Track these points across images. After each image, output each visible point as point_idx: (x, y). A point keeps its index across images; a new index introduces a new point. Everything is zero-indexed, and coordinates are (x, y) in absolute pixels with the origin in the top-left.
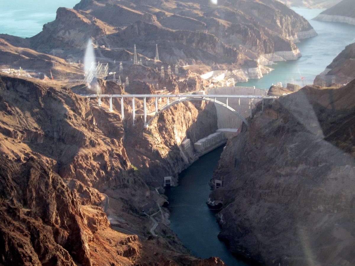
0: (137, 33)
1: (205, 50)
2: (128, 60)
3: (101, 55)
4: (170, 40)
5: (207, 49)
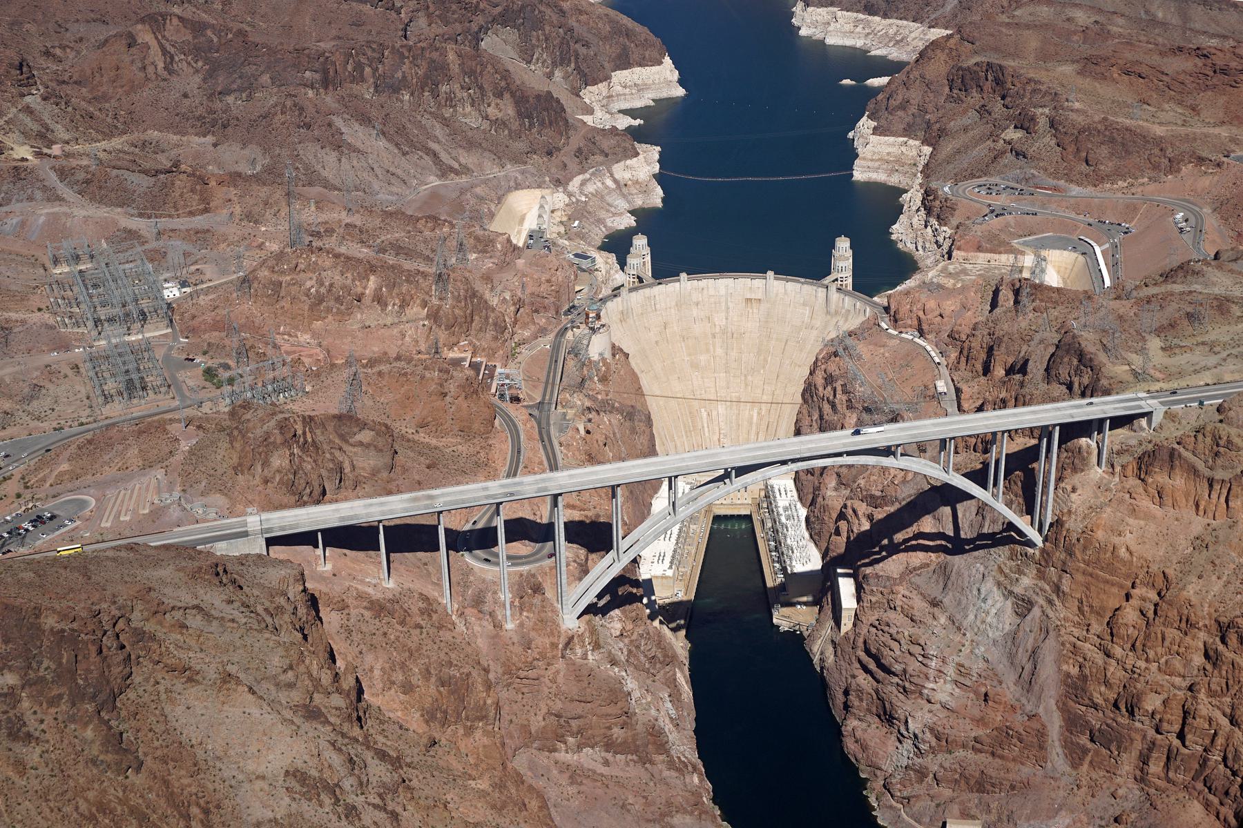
0: (161, 65)
1: (447, 113)
2: (206, 210)
3: (63, 190)
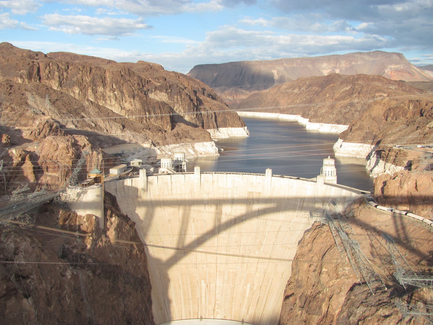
1: (101, 103)
4: (21, 77)
5: (105, 100)
